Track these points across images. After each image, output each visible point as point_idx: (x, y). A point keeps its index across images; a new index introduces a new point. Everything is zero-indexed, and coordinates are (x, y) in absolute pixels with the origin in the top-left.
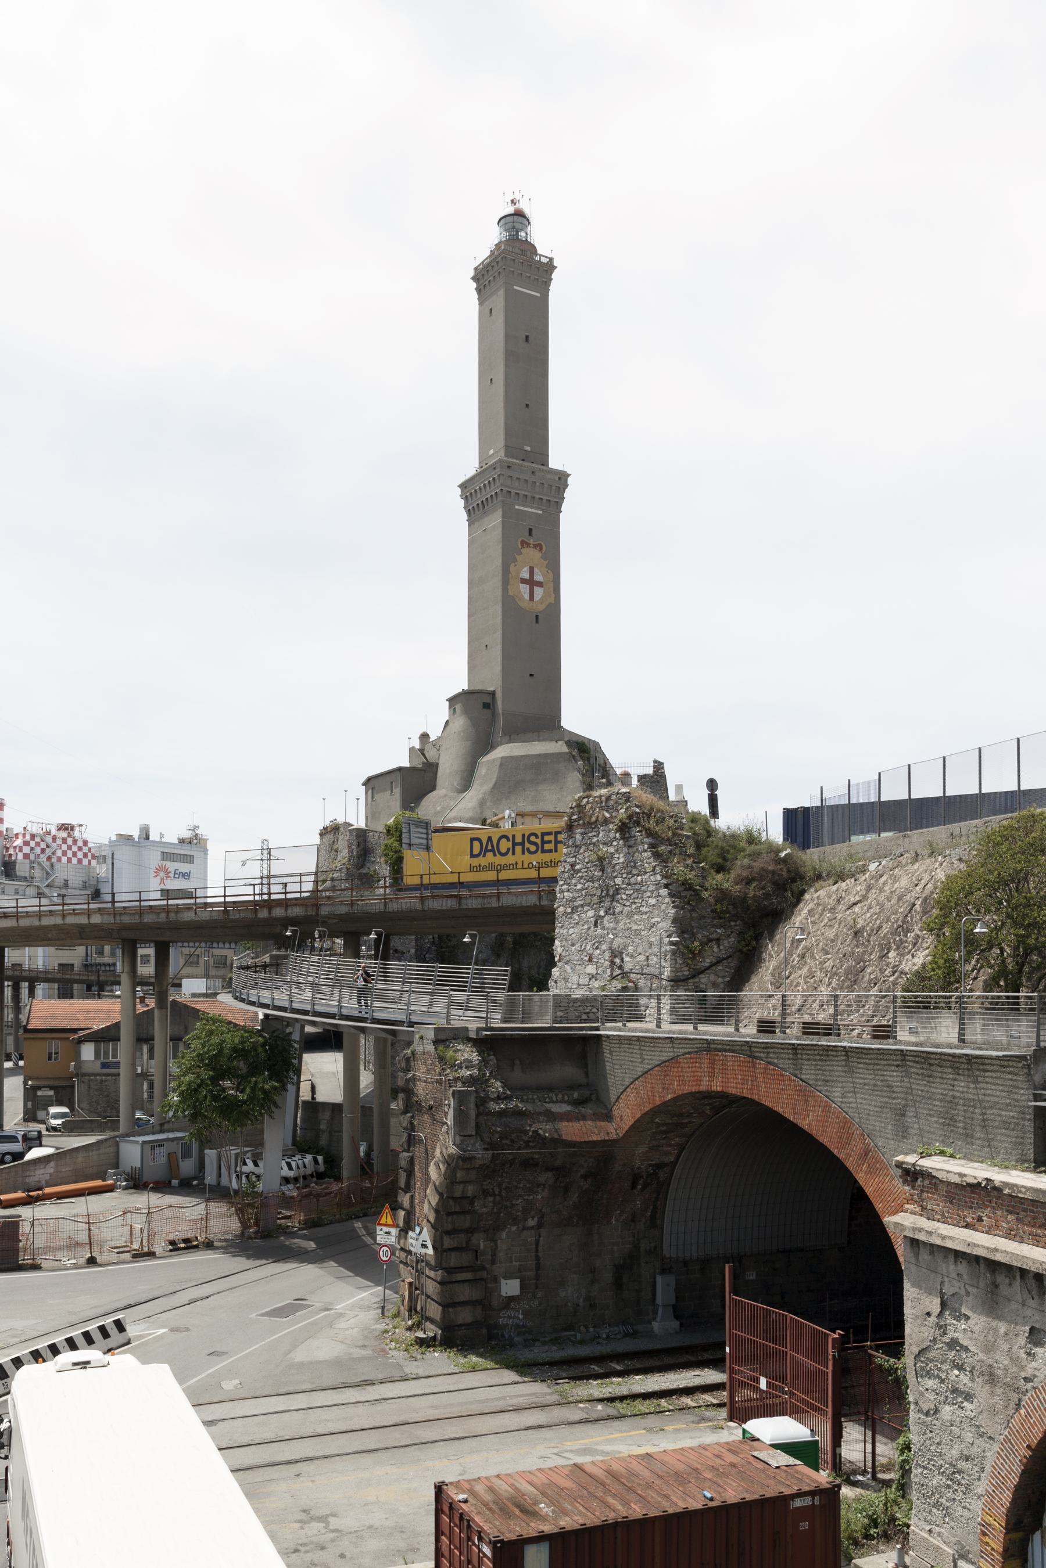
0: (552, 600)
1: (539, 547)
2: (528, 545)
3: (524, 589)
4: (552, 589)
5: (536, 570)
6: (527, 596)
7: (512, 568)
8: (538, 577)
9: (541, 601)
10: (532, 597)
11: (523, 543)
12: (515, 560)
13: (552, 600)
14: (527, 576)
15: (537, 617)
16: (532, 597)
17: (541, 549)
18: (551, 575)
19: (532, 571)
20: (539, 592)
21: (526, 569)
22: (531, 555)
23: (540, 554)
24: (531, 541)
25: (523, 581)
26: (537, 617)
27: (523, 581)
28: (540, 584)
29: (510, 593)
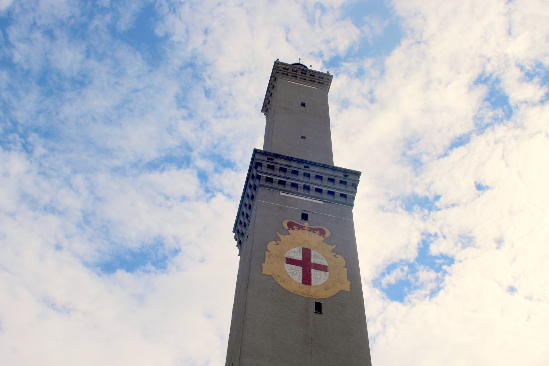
0: (346, 286)
3: (295, 273)
4: (344, 275)
5: (313, 253)
9: (326, 286)
10: (307, 279)
12: (277, 239)
13: (346, 286)
14: (299, 257)
16: (307, 279)
17: (322, 233)
18: (341, 261)
19: (306, 253)
23: (321, 238)
25: (290, 261)
27: (290, 261)
29: (265, 272)
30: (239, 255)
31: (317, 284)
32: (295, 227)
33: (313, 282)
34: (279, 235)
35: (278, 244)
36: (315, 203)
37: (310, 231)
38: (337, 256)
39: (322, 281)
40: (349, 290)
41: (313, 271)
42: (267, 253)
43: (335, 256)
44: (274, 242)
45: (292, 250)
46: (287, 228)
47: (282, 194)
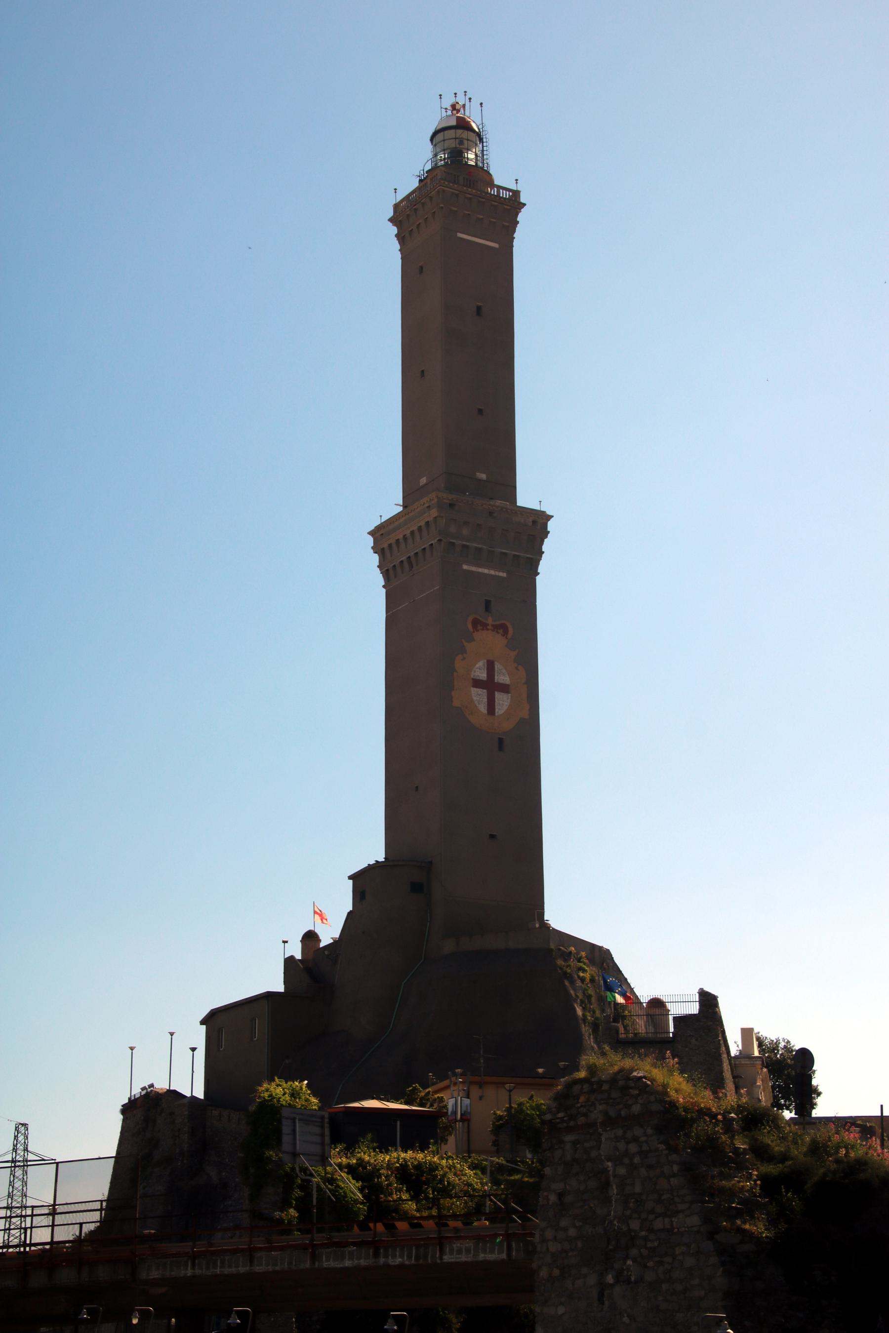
1: (501, 629)
2: (485, 626)
3: (479, 696)
5: (497, 666)
6: (483, 708)
7: (459, 663)
8: (502, 677)
11: (476, 623)
13: (525, 713)
14: (483, 676)
15: (501, 741)
19: (490, 667)
20: (503, 702)
21: (481, 664)
22: (490, 642)
24: (490, 621)
25: (477, 683)
26: (501, 741)
27: (477, 683)
28: (504, 688)
29: (456, 703)
30: (384, 586)
31: (501, 712)
32: (479, 627)
33: (497, 710)
34: (466, 644)
35: (464, 658)
36: (499, 576)
37: (493, 631)
38: (520, 667)
39: (505, 708)
40: (527, 717)
41: (497, 695)
42: (455, 674)
43: (517, 668)
44: (460, 657)
45: (477, 666)
46: (471, 629)
47: (465, 567)
